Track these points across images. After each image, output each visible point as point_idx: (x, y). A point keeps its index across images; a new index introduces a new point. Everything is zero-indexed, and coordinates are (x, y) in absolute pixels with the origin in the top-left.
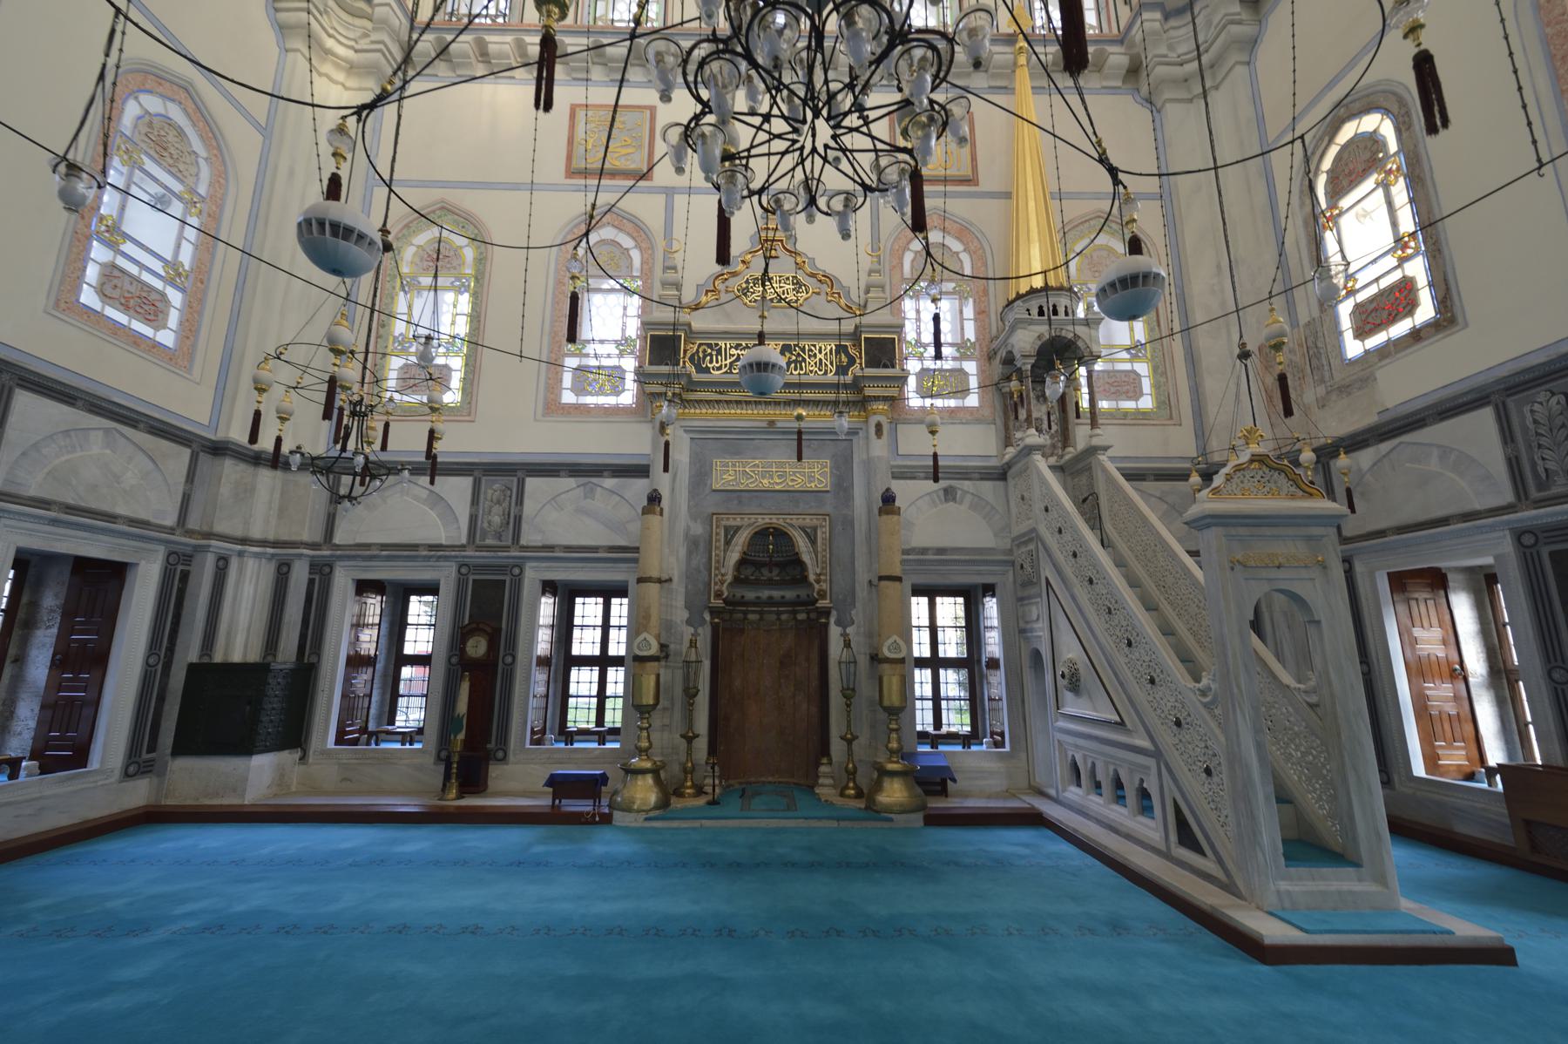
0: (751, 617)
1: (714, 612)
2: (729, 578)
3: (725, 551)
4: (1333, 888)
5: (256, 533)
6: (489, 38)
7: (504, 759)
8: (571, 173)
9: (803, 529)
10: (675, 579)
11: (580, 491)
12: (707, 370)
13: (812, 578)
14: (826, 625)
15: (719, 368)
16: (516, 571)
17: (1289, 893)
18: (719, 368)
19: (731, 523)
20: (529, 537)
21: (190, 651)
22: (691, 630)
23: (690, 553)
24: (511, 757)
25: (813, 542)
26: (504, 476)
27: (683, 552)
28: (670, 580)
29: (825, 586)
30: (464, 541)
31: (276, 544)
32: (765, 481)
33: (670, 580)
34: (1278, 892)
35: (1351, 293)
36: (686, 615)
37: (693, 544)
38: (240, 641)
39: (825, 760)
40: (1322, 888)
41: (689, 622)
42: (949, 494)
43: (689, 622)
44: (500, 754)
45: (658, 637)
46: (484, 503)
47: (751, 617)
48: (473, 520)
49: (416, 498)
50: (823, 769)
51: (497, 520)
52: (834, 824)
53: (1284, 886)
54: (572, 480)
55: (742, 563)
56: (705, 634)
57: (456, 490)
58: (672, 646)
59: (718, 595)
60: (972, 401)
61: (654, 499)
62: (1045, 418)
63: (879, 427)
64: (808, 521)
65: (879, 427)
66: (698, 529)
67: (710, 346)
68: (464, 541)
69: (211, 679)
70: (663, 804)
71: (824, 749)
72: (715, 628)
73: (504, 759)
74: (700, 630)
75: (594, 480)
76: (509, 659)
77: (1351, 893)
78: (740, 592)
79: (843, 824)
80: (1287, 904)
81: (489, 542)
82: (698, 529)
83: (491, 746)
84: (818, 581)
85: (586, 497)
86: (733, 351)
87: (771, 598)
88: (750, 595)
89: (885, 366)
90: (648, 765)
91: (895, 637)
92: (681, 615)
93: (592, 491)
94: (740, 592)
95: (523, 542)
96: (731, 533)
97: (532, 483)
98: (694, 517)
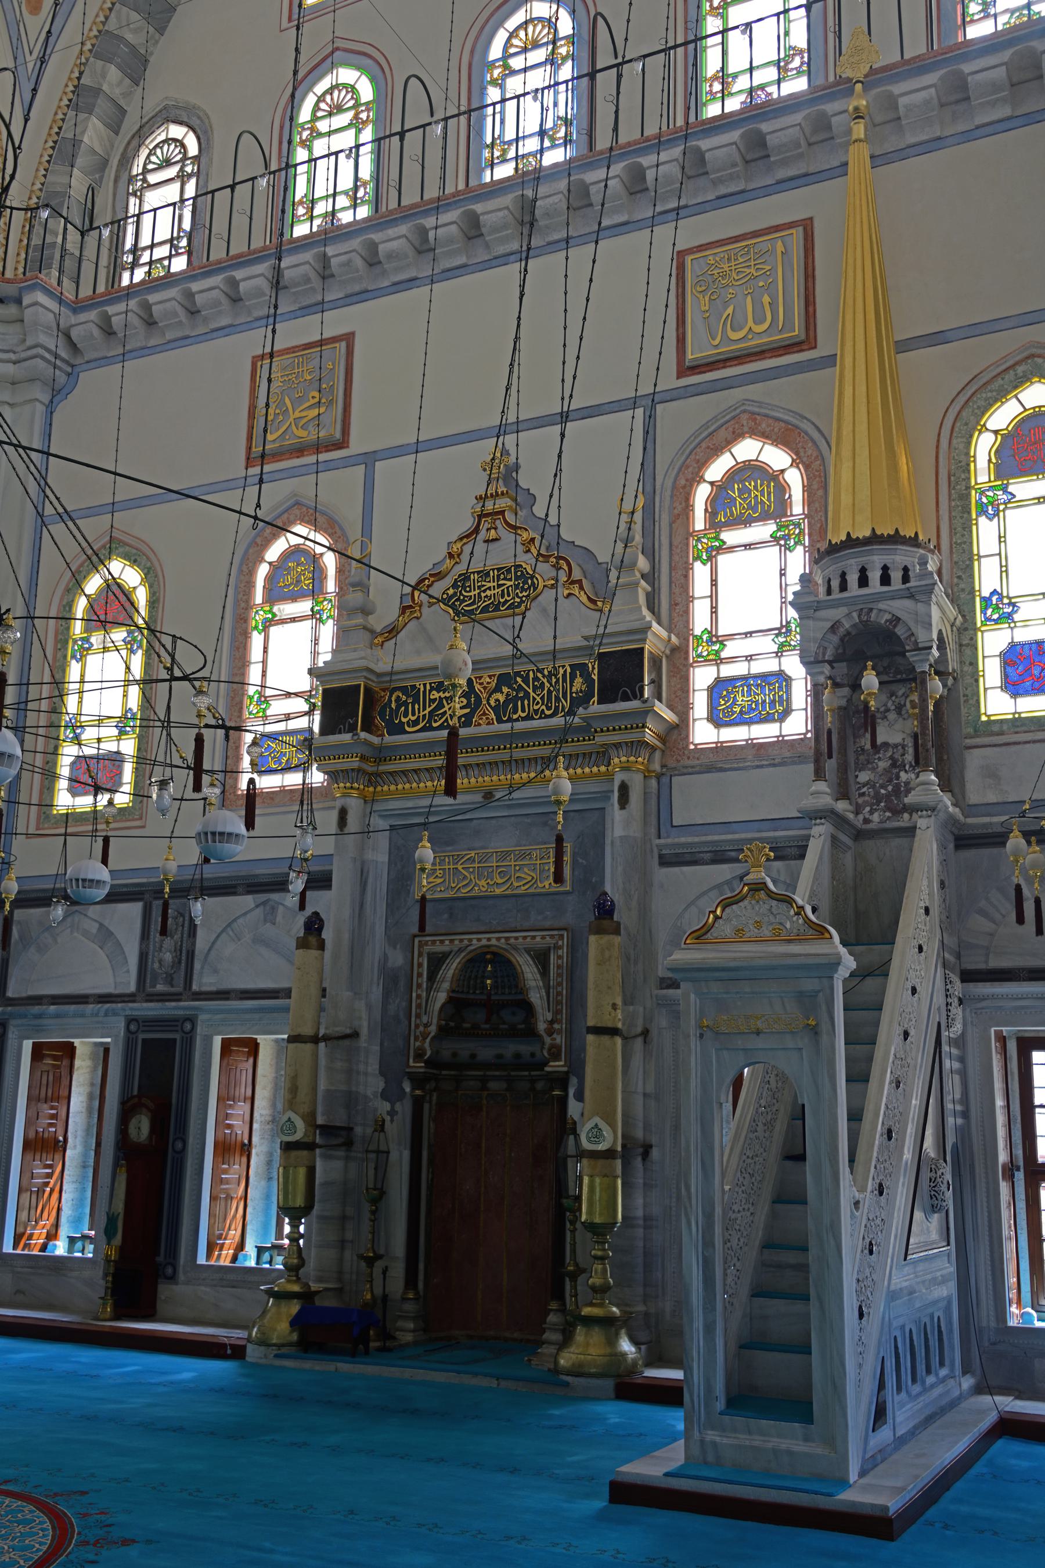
0: (493, 1085)
1: (418, 1081)
2: (433, 1029)
3: (429, 990)
4: (784, 1446)
6: (152, 298)
7: (173, 1278)
9: (528, 951)
10: (364, 1032)
11: (259, 911)
12: (400, 729)
13: (542, 1026)
14: (563, 1102)
15: (416, 723)
16: (188, 1026)
17: (714, 1444)
18: (416, 723)
19: (438, 948)
20: (205, 980)
22: (387, 1106)
23: (386, 995)
24: (181, 1277)
25: (544, 972)
27: (376, 993)
28: (355, 1035)
29: (559, 1039)
30: (132, 988)
32: (483, 883)
33: (355, 1035)
34: (702, 1441)
36: (381, 1085)
37: (391, 980)
39: (554, 1305)
40: (756, 1443)
41: (385, 1095)
43: (385, 1095)
44: (169, 1271)
45: (310, 1118)
47: (493, 1085)
48: (143, 958)
49: (86, 933)
50: (552, 1318)
51: (168, 957)
52: (494, 1383)
53: (712, 1436)
54: (249, 898)
55: (456, 1004)
56: (405, 1108)
58: (358, 1130)
59: (419, 1055)
61: (314, 926)
62: (910, 742)
63: (624, 789)
64: (540, 940)
65: (624, 789)
66: (397, 959)
67: (404, 690)
68: (132, 988)
72: (418, 1104)
73: (173, 1278)
74: (398, 1106)
75: (275, 896)
76: (179, 1145)
77: (790, 1453)
78: (464, 1048)
79: (504, 1384)
80: (710, 1458)
81: (160, 988)
83: (160, 1259)
84: (550, 1032)
85: (265, 921)
86: (435, 695)
87: (518, 1056)
88: (486, 1052)
89: (626, 698)
90: (296, 1288)
91: (597, 1120)
92: (372, 1084)
93: (274, 909)
94: (464, 1048)
95: (195, 987)
96: (437, 962)
98: (391, 941)
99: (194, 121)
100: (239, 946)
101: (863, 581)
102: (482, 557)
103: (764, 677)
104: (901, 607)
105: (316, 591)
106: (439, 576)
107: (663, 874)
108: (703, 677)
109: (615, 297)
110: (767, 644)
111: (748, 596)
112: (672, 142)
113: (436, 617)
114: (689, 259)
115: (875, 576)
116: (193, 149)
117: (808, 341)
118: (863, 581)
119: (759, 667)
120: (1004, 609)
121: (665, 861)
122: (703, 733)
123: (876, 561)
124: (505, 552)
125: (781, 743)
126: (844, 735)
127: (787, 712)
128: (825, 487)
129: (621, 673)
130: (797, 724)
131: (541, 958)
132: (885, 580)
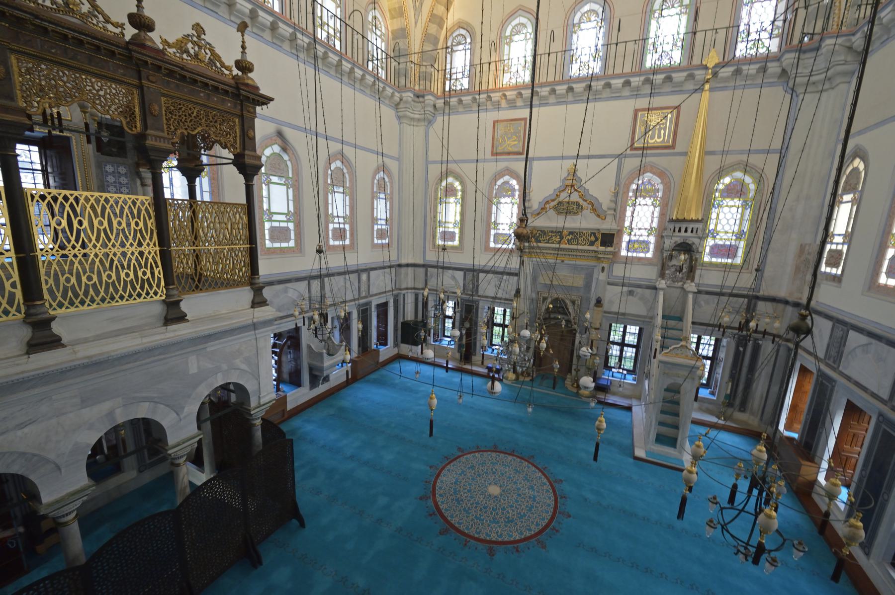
5: (409, 286)
8: (493, 154)
20: (480, 293)
21: (401, 320)
26: (473, 273)
31: (414, 288)
35: (832, 243)
38: (410, 317)
42: (631, 293)
46: (467, 281)
48: (464, 285)
57: (459, 275)
60: (649, 255)
69: (405, 325)
70: (517, 379)
71: (570, 371)
82: (534, 296)
97: (482, 275)
99: (469, 29)
100: (488, 286)
101: (686, 231)
102: (564, 196)
103: (643, 241)
104: (696, 241)
105: (513, 196)
106: (553, 200)
107: (609, 287)
108: (626, 238)
109: (612, 119)
110: (645, 233)
111: (642, 219)
112: (643, 75)
113: (552, 213)
114: (640, 114)
115: (689, 230)
116: (469, 40)
117: (673, 147)
118: (686, 231)
119: (641, 239)
120: (714, 234)
121: (609, 284)
122: (624, 253)
123: (690, 226)
124: (575, 197)
125: (645, 259)
126: (663, 261)
127: (648, 251)
128: (670, 191)
129: (609, 239)
130: (649, 255)
131: (573, 302)
132: (692, 231)
